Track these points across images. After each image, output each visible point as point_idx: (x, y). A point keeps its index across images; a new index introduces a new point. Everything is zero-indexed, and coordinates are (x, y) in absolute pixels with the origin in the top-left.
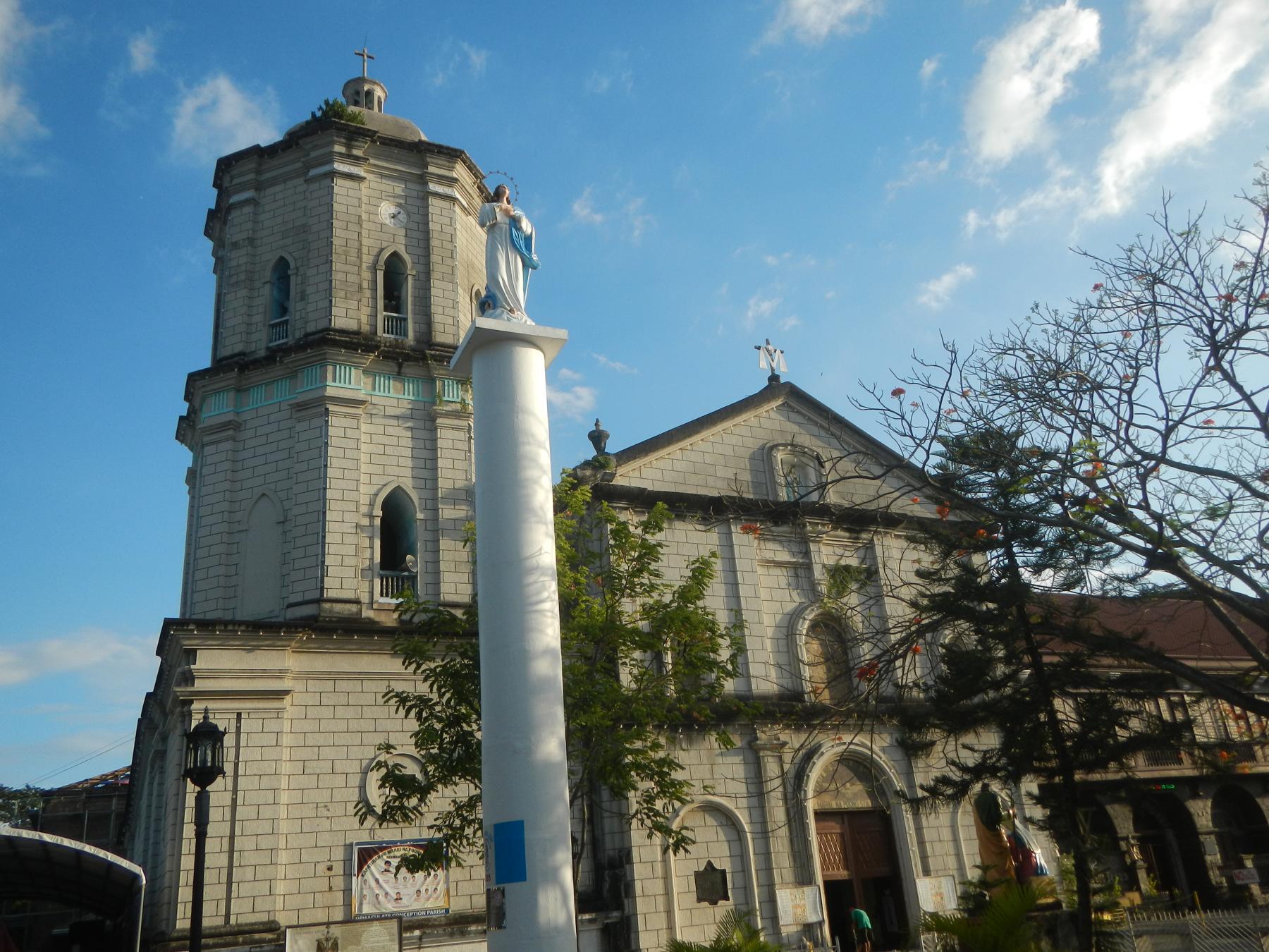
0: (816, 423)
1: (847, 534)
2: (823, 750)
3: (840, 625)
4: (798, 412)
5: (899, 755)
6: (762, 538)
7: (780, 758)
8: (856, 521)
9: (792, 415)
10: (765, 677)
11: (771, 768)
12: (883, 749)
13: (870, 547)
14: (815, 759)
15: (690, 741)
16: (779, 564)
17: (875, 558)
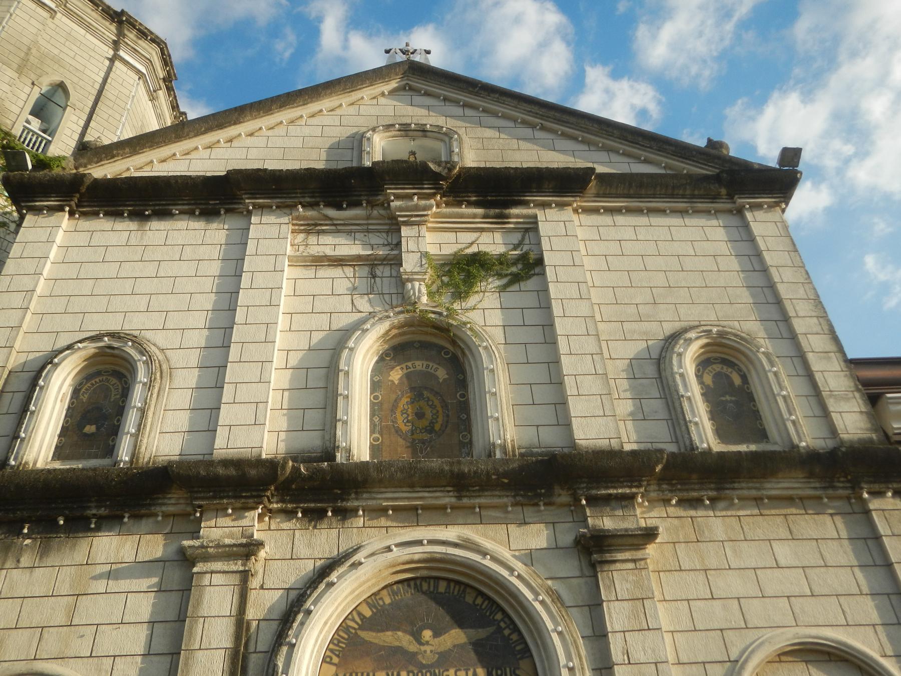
0: (456, 102)
1: (480, 211)
2: (359, 557)
3: (454, 343)
4: (427, 94)
5: (570, 567)
6: (312, 228)
7: (245, 576)
8: (496, 191)
9: (418, 99)
10: (259, 428)
11: (216, 597)
12: (529, 558)
13: (531, 228)
14: (333, 577)
15: (44, 551)
16: (339, 262)
17: (539, 244)
